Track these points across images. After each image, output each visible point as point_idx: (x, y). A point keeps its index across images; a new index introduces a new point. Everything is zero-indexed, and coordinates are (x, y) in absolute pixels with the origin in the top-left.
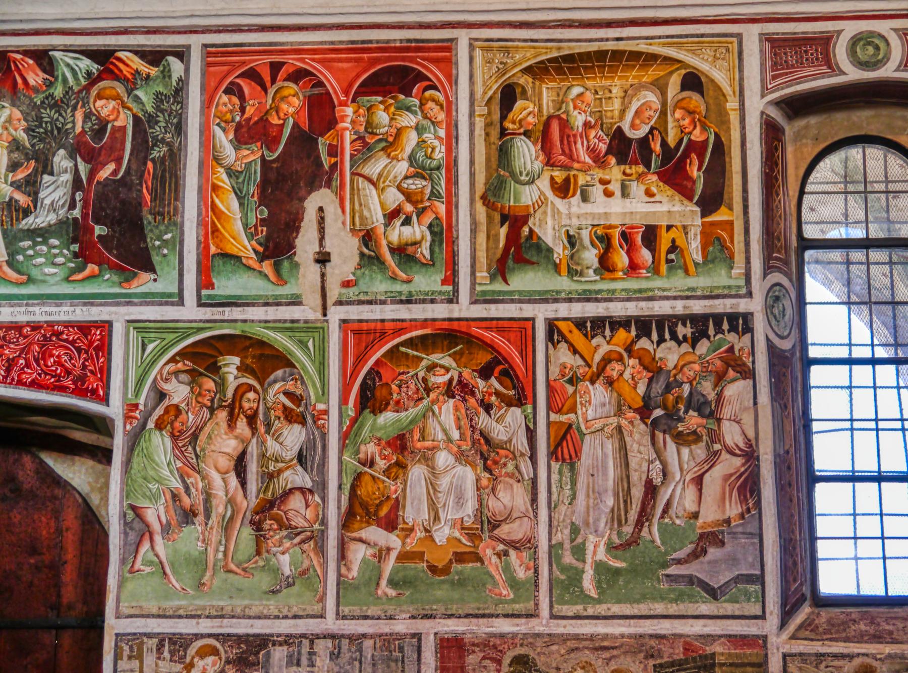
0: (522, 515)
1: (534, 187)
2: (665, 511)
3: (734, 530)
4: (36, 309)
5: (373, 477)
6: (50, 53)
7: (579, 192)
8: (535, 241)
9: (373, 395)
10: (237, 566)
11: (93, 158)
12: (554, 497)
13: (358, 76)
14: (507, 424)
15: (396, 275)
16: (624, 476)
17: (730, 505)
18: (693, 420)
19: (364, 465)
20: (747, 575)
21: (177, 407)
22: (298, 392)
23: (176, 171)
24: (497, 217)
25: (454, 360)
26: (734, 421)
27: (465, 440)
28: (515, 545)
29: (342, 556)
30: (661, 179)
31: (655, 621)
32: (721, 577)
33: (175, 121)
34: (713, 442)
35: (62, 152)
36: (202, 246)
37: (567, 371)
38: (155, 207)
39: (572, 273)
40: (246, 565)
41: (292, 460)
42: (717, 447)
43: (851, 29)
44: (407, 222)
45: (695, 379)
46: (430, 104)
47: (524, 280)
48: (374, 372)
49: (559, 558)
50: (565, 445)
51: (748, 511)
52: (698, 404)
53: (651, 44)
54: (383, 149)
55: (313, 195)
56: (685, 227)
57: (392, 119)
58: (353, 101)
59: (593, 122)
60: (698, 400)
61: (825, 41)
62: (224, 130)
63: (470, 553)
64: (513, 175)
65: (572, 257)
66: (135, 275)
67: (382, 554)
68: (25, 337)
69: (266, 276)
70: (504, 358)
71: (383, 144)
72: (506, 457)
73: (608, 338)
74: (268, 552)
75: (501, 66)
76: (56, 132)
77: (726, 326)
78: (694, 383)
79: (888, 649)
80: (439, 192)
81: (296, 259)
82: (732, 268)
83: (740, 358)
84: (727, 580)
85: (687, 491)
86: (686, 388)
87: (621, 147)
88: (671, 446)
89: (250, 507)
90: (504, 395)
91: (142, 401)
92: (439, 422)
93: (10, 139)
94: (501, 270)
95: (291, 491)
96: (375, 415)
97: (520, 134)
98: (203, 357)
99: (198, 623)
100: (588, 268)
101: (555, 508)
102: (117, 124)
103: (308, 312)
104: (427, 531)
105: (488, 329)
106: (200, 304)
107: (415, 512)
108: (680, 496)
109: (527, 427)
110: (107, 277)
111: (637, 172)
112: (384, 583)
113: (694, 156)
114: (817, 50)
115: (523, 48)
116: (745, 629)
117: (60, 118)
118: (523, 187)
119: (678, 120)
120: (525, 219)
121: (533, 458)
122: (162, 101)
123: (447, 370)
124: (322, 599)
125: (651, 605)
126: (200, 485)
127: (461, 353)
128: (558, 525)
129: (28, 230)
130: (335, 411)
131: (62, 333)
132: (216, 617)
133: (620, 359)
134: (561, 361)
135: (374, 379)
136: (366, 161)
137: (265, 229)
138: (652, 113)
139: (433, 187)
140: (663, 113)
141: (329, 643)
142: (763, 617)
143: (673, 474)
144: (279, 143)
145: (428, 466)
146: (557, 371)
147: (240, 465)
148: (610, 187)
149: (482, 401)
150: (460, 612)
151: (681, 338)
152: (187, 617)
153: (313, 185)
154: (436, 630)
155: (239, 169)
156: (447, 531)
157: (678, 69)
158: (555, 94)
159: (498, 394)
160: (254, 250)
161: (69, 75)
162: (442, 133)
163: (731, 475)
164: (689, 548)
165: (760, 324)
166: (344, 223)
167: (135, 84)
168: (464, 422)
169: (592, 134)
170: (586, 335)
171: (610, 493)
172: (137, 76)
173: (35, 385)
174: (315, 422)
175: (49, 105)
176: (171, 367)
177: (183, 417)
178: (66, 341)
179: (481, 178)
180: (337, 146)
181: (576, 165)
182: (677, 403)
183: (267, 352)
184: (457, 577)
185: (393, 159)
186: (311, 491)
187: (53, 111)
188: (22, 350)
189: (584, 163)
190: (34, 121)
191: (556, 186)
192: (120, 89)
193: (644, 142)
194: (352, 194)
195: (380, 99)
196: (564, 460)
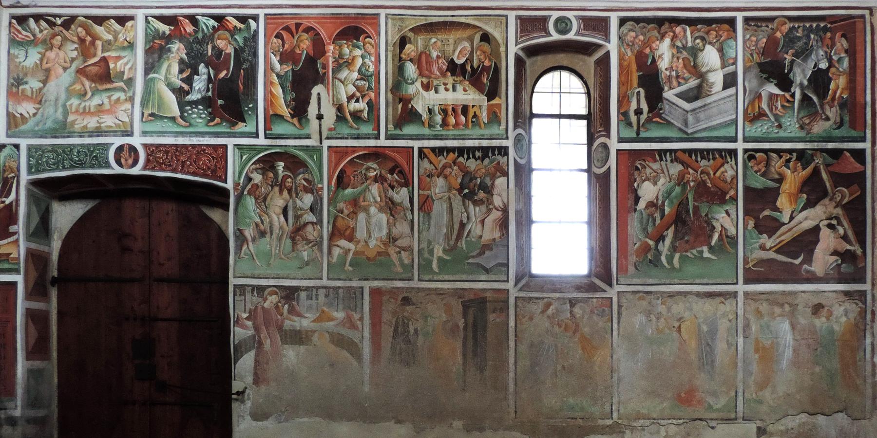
2: (468, 235)
4: (194, 139)
18: (481, 195)
21: (257, 185)
28: (404, 249)
35: (202, 65)
39: (430, 126)
42: (491, 207)
43: (555, 15)
44: (357, 101)
46: (368, 45)
47: (409, 130)
48: (342, 172)
50: (426, 204)
52: (484, 188)
56: (480, 106)
57: (351, 52)
61: (544, 20)
66: (237, 124)
77: (496, 152)
79: (558, 295)
86: (479, 180)
87: (453, 68)
88: (471, 206)
91: (241, 181)
94: (398, 125)
95: (308, 223)
98: (268, 163)
105: (393, 151)
106: (266, 138)
107: (361, 234)
108: (474, 228)
112: (347, 264)
120: (409, 100)
121: (412, 210)
123: (375, 170)
124: (322, 271)
130: (325, 187)
133: (451, 167)
140: (472, 52)
141: (324, 290)
142: (507, 281)
147: (285, 212)
153: (315, 83)
156: (374, 242)
159: (397, 181)
161: (205, 28)
162: (373, 59)
164: (477, 251)
165: (511, 152)
168: (383, 194)
169: (440, 61)
173: (194, 174)
176: (254, 167)
179: (390, 81)
186: (316, 224)
192: (228, 35)
193: (463, 66)
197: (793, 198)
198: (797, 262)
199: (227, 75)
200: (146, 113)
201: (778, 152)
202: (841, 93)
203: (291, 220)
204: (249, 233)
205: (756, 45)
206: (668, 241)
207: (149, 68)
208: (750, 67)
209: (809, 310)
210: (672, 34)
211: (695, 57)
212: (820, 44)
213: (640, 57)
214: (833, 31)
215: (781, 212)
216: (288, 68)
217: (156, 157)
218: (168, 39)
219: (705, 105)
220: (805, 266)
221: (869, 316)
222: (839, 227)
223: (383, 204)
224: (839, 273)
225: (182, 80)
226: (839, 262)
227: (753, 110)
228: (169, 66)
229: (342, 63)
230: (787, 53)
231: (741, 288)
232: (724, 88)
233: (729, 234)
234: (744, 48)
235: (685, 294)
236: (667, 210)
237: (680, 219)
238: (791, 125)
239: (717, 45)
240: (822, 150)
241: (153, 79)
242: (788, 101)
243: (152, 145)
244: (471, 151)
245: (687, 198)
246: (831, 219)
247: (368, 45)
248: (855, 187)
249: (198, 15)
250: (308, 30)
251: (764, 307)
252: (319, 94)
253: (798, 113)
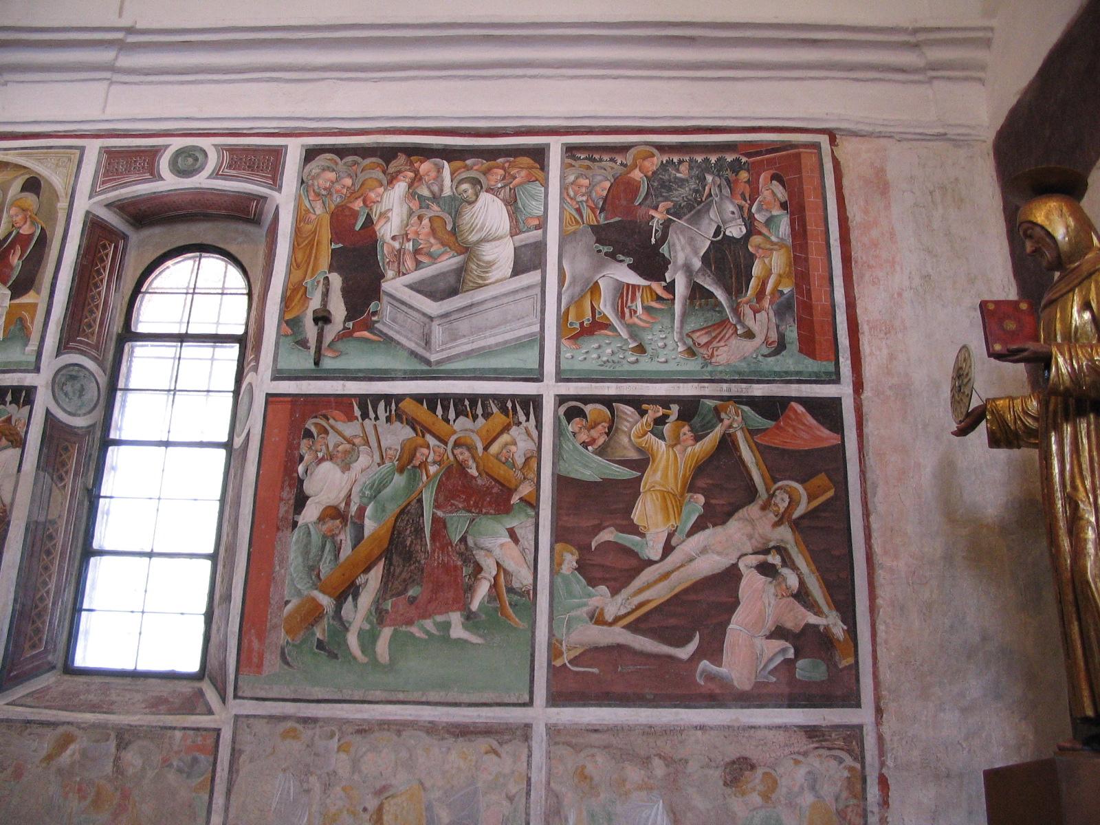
43: (177, 143)
61: (154, 153)
77: (9, 398)
82: (26, 345)
113: (18, 248)
114: (145, 160)
119: (12, 217)
157: (22, 174)
165: (43, 399)
197: (673, 503)
198: (684, 653)
201: (637, 403)
202: (778, 283)
205: (589, 194)
206: (366, 599)
208: (574, 233)
209: (716, 775)
210: (411, 175)
211: (457, 214)
212: (726, 191)
213: (341, 220)
214: (755, 170)
215: (643, 535)
219: (471, 306)
220: (705, 664)
221: (873, 792)
222: (785, 571)
224: (792, 681)
226: (791, 654)
227: (580, 315)
230: (656, 208)
231: (542, 715)
232: (516, 272)
233: (516, 585)
234: (562, 199)
235: (399, 727)
236: (369, 526)
237: (398, 549)
238: (667, 345)
239: (505, 193)
240: (739, 400)
242: (659, 299)
245: (420, 501)
246: (766, 551)
248: (821, 479)
251: (599, 766)
253: (682, 322)
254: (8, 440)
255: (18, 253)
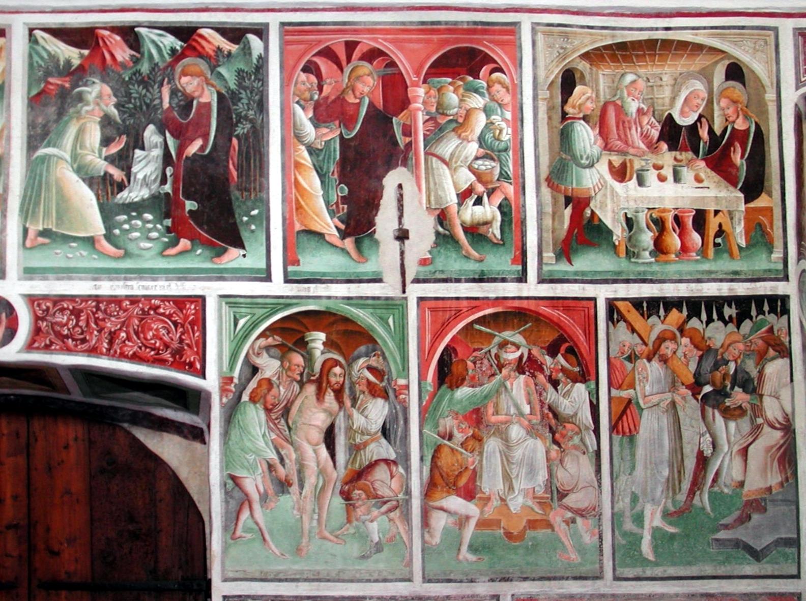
0: (588, 485)
1: (593, 169)
2: (715, 480)
3: (776, 498)
5: (452, 450)
6: (136, 29)
7: (635, 176)
8: (596, 223)
9: (450, 370)
10: (331, 533)
11: (182, 135)
12: (616, 469)
13: (428, 57)
14: (573, 399)
15: (470, 254)
16: (678, 448)
17: (772, 475)
18: (739, 397)
19: (443, 438)
20: (786, 539)
21: (269, 381)
22: (380, 367)
23: (260, 148)
24: (562, 200)
25: (525, 337)
26: (774, 396)
27: (535, 415)
28: (581, 513)
29: (426, 523)
30: (708, 165)
31: (706, 581)
32: (763, 541)
33: (257, 98)
34: (756, 416)
35: (151, 127)
36: (287, 222)
37: (626, 349)
38: (242, 182)
39: (630, 254)
40: (339, 532)
41: (376, 433)
42: (760, 421)
44: (479, 202)
45: (739, 357)
46: (497, 87)
47: (589, 261)
49: (621, 524)
50: (625, 418)
51: (787, 479)
53: (696, 35)
54: (454, 130)
55: (391, 173)
56: (730, 213)
57: (461, 101)
58: (425, 82)
59: (646, 109)
60: (743, 377)
62: (303, 108)
63: (541, 520)
64: (574, 158)
65: (630, 238)
66: (225, 251)
67: (463, 521)
68: (125, 310)
69: (348, 253)
70: (569, 336)
71: (454, 125)
72: (572, 431)
73: (662, 318)
74: (357, 520)
75: (561, 51)
76: (144, 108)
77: (766, 308)
78: (739, 361)
80: (507, 173)
81: (376, 236)
82: (771, 252)
83: (779, 337)
84: (768, 543)
85: (734, 462)
86: (732, 367)
87: (672, 134)
88: (719, 420)
89: (339, 478)
90: (570, 371)
91: (236, 374)
92: (512, 398)
93: (102, 114)
94: (565, 251)
95: (377, 462)
96: (452, 390)
97: (579, 119)
98: (291, 332)
99: (297, 586)
100: (644, 250)
101: (617, 478)
102: (203, 100)
103: (388, 289)
104: (502, 500)
106: (287, 281)
108: (727, 465)
109: (591, 402)
110: (199, 251)
111: (687, 158)
112: (464, 548)
113: (737, 145)
115: (581, 34)
116: (783, 587)
117: (148, 94)
118: (583, 170)
120: (586, 202)
121: (597, 431)
122: (243, 78)
123: (518, 347)
124: (410, 563)
125: (702, 568)
126: (294, 456)
127: (530, 330)
128: (619, 495)
129: (123, 204)
130: (414, 381)
131: (159, 307)
132: (313, 580)
133: (673, 338)
134: (620, 340)
135: (451, 356)
136: (439, 140)
137: (346, 206)
138: (699, 101)
139: (501, 168)
140: (710, 102)
143: (722, 446)
144: (356, 122)
145: (502, 439)
146: (617, 349)
148: (663, 172)
149: (550, 376)
150: (534, 575)
151: (727, 318)
152: (286, 580)
153: (390, 165)
154: (513, 592)
155: (319, 147)
156: (520, 500)
157: (722, 59)
158: (610, 80)
159: (563, 370)
160: (337, 227)
161: (154, 52)
162: (508, 115)
163: (772, 447)
164: (736, 514)
166: (421, 203)
167: (217, 61)
168: (535, 398)
169: (645, 120)
170: (642, 315)
171: (666, 464)
172: (219, 52)
173: (136, 358)
174: (396, 397)
175: (136, 81)
176: (262, 342)
177: (274, 391)
178: (163, 314)
179: (545, 160)
180: (410, 126)
181: (631, 151)
182: (724, 379)
183: (350, 328)
184: (530, 543)
185: (463, 139)
187: (141, 87)
188: (123, 323)
189: (638, 148)
190: (123, 97)
191: (614, 170)
192: (203, 65)
193: (693, 129)
194: (427, 173)
195: (449, 80)
196: (624, 433)
199: (202, 148)
200: (33, 229)
203: (341, 456)
204: (254, 483)
207: (38, 136)
216: (331, 134)
217: (53, 324)
218: (79, 74)
223: (536, 420)
225: (110, 159)
228: (81, 132)
229: (444, 125)
241: (45, 159)
243: (45, 297)
244: (714, 304)
247: (497, 87)
249: (140, 25)
250: (372, 55)
252: (400, 186)
254: (776, 351)
255: (739, 150)
